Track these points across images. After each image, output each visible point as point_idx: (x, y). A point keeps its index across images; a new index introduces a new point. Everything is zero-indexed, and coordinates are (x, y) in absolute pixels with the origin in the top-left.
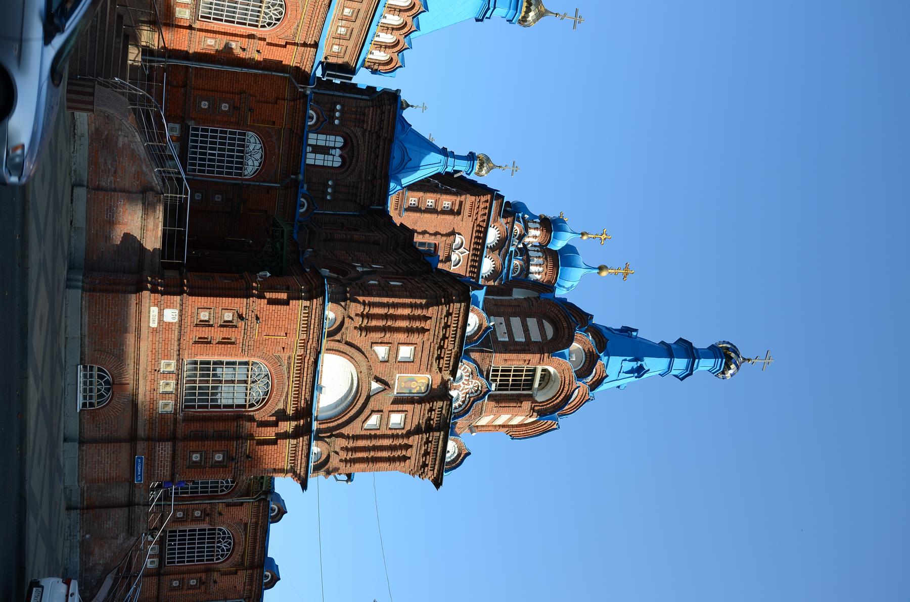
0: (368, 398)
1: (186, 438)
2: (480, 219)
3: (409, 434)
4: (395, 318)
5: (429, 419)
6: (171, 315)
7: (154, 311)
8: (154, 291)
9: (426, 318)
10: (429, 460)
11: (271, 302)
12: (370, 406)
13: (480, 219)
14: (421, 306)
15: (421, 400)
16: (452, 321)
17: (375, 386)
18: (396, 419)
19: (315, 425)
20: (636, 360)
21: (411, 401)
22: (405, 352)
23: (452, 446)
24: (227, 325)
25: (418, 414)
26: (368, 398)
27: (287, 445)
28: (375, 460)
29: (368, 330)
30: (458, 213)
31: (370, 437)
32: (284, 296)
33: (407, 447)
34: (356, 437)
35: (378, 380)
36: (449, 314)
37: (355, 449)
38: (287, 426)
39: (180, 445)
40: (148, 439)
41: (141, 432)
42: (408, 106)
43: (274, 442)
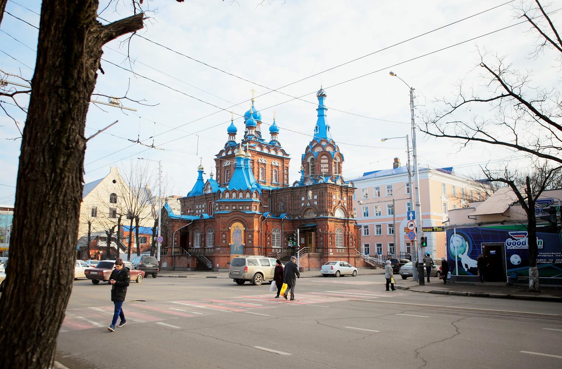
0: (342, 206)
1: (348, 246)
2: (255, 154)
3: (347, 196)
4: (329, 200)
5: (345, 191)
6: (331, 250)
7: (331, 254)
8: (328, 254)
9: (329, 193)
10: (352, 191)
11: (328, 229)
12: (343, 205)
13: (255, 154)
14: (327, 194)
15: (342, 193)
16: (330, 187)
17: (340, 205)
18: (345, 199)
19: (346, 218)
20: (326, 128)
21: (342, 195)
22: (334, 197)
23: (350, 185)
24: (332, 239)
25: (344, 194)
26: (342, 206)
27: (350, 225)
28: (352, 204)
29: (331, 207)
30: (253, 161)
31: (348, 205)
32: (327, 226)
33: (350, 196)
34: (348, 209)
35: (339, 204)
36: (329, 188)
37: (350, 208)
38: (346, 224)
39: (350, 248)
40: (349, 254)
41: (348, 256)
42: (211, 173)
43: (349, 227)
